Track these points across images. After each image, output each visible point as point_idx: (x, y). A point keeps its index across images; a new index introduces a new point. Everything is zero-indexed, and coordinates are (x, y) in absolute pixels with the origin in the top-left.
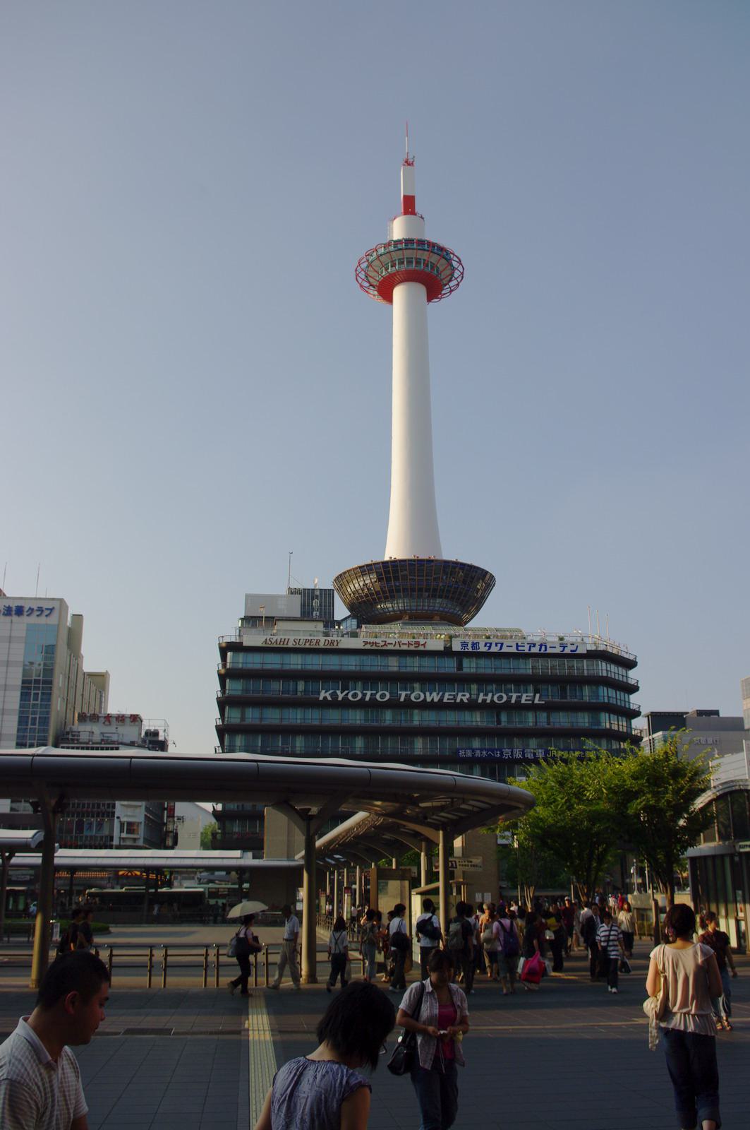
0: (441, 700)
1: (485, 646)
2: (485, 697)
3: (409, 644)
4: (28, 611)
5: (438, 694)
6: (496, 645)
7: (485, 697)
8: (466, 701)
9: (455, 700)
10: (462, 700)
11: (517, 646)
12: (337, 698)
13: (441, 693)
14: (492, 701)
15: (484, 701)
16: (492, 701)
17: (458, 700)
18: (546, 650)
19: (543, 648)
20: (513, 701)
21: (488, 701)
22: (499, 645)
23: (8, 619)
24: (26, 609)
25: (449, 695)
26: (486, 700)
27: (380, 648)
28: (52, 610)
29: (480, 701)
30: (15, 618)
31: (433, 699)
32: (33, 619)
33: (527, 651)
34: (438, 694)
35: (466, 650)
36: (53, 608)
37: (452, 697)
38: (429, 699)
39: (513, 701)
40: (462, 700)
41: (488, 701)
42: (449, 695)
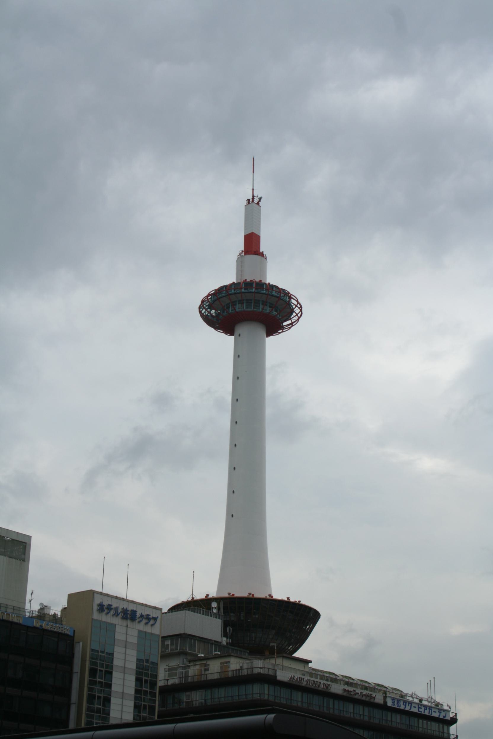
1: (403, 704)
3: (367, 696)
4: (139, 618)
6: (409, 705)
11: (419, 708)
18: (431, 714)
19: (430, 713)
22: (410, 705)
23: (124, 623)
24: (138, 614)
27: (351, 696)
28: (155, 619)
30: (129, 621)
32: (141, 627)
33: (423, 713)
35: (394, 706)
36: (158, 617)
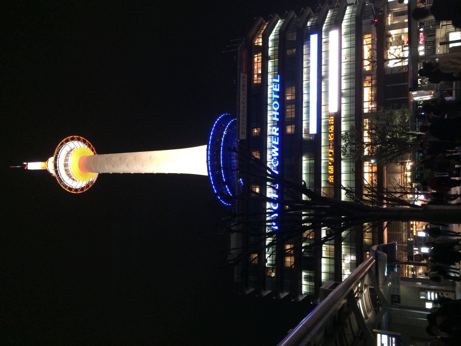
0: (277, 146)
2: (275, 116)
5: (274, 148)
7: (275, 116)
8: (278, 129)
9: (278, 136)
10: (277, 132)
12: (276, 216)
13: (273, 147)
14: (278, 111)
15: (278, 116)
16: (278, 111)
17: (278, 134)
20: (278, 97)
21: (278, 114)
25: (274, 140)
26: (277, 115)
29: (278, 119)
31: (277, 152)
34: (274, 148)
37: (275, 138)
38: (277, 154)
39: (278, 97)
40: (277, 132)
41: (278, 114)
42: (274, 140)
